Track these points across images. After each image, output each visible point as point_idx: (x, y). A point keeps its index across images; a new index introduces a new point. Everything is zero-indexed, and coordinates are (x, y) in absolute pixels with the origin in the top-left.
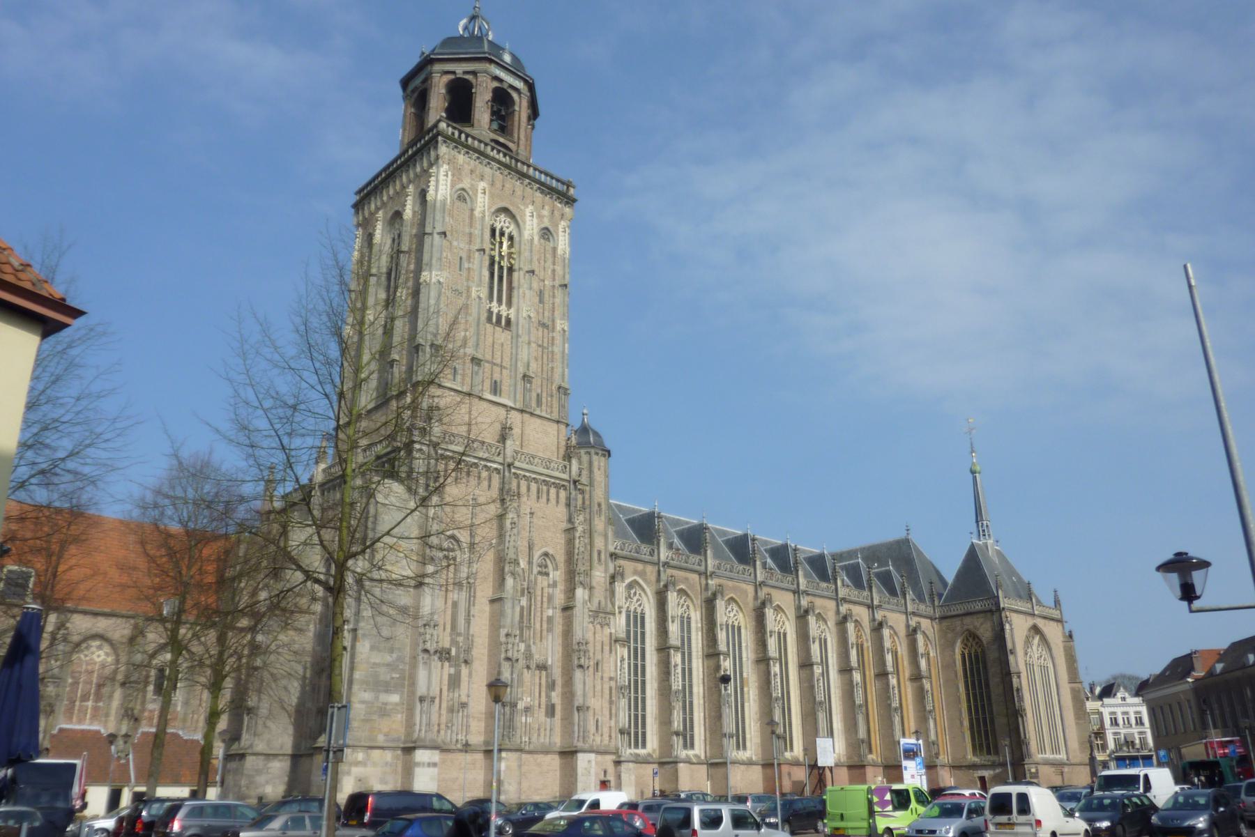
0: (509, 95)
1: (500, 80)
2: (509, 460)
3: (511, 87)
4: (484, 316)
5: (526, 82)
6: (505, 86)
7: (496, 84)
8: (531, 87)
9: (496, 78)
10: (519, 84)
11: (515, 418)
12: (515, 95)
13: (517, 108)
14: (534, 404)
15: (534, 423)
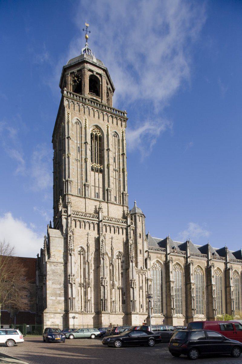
0: (97, 77)
1: (92, 71)
2: (100, 219)
3: (97, 73)
4: (89, 169)
5: (104, 70)
6: (95, 73)
7: (91, 73)
8: (105, 71)
9: (90, 70)
10: (101, 72)
11: (104, 205)
12: (98, 76)
13: (101, 83)
14: (113, 200)
15: (112, 208)
